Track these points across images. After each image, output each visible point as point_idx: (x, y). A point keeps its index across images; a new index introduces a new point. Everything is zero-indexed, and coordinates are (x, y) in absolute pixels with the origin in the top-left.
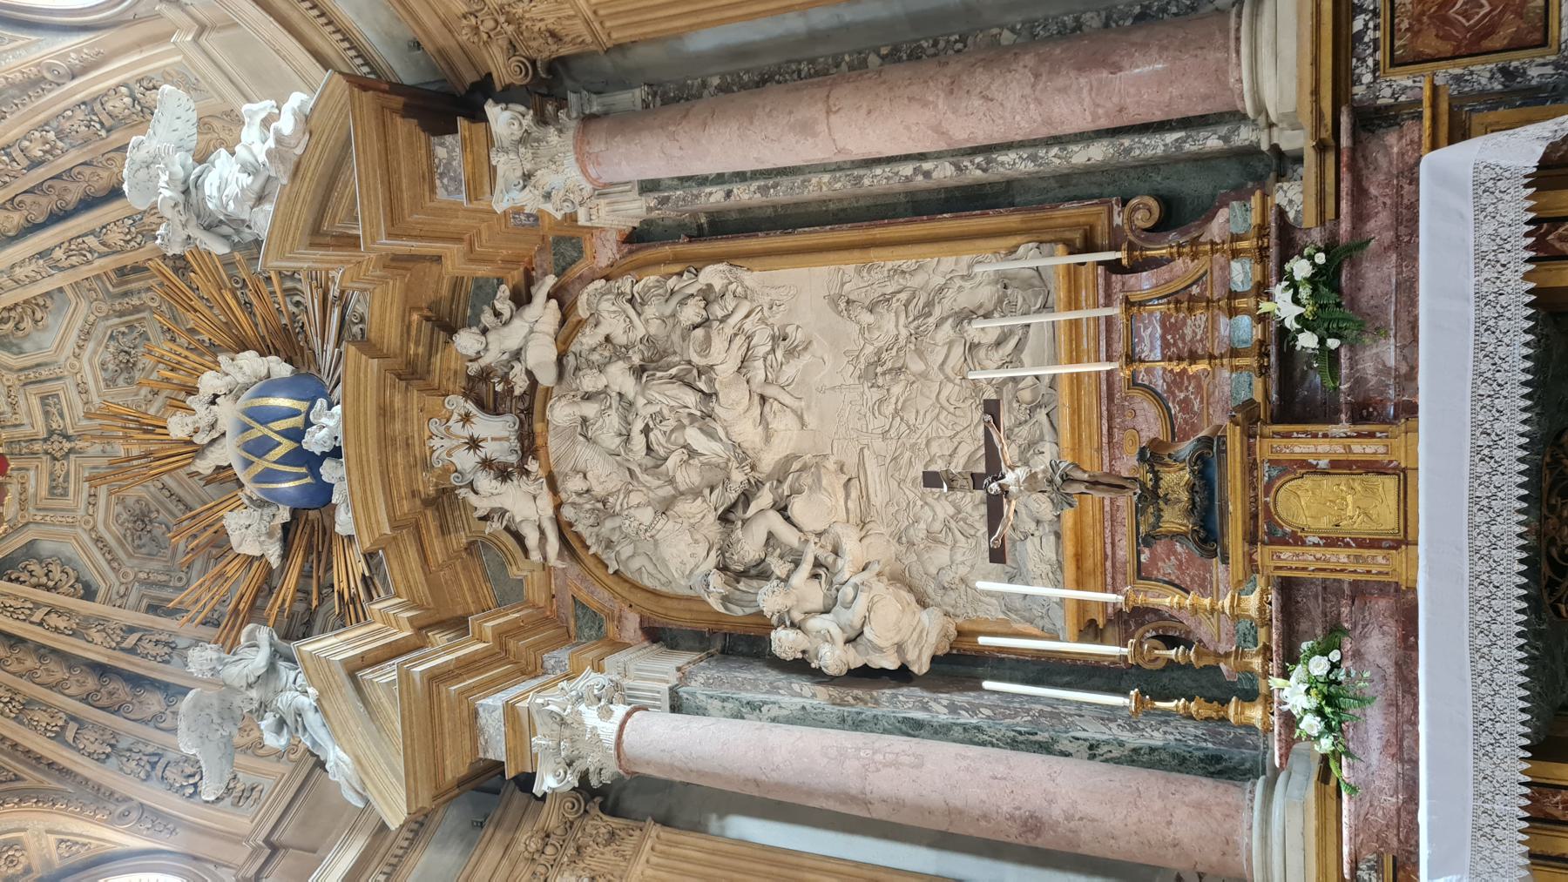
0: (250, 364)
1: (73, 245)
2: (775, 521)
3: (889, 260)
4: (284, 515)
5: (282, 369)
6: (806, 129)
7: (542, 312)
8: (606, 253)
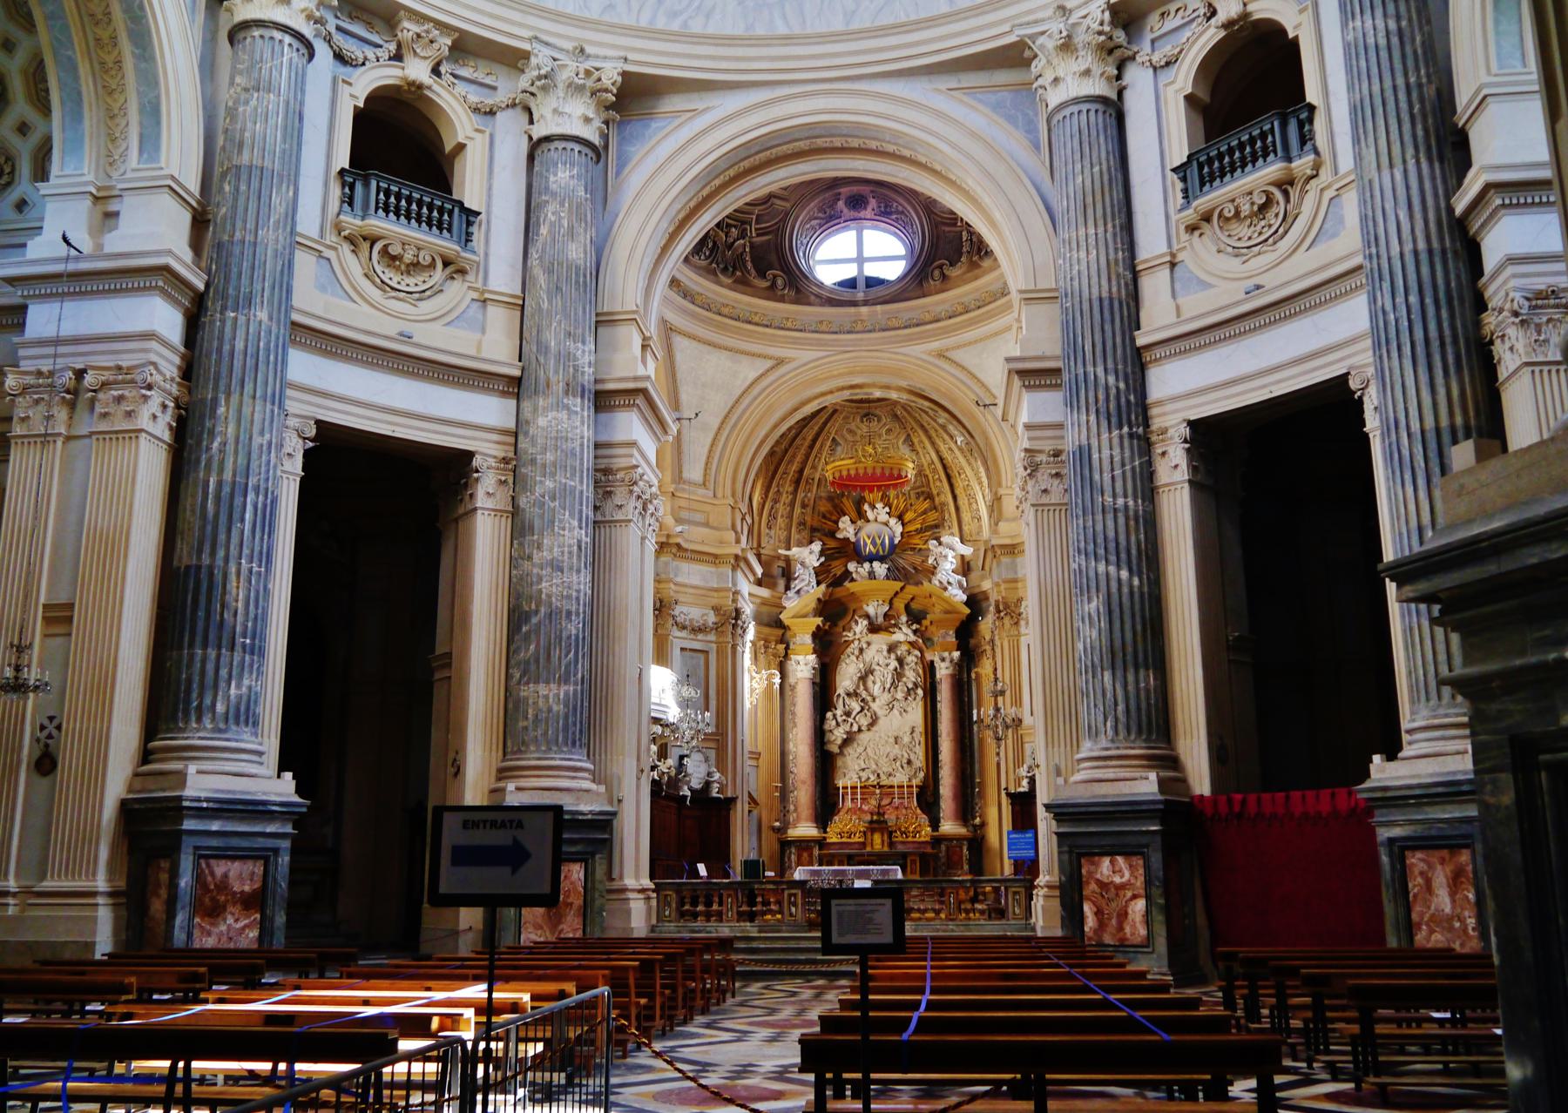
0: (899, 529)
1: (935, 471)
2: (858, 709)
3: (923, 740)
4: (853, 539)
5: (896, 541)
6: (948, 735)
7: (912, 638)
8: (928, 657)
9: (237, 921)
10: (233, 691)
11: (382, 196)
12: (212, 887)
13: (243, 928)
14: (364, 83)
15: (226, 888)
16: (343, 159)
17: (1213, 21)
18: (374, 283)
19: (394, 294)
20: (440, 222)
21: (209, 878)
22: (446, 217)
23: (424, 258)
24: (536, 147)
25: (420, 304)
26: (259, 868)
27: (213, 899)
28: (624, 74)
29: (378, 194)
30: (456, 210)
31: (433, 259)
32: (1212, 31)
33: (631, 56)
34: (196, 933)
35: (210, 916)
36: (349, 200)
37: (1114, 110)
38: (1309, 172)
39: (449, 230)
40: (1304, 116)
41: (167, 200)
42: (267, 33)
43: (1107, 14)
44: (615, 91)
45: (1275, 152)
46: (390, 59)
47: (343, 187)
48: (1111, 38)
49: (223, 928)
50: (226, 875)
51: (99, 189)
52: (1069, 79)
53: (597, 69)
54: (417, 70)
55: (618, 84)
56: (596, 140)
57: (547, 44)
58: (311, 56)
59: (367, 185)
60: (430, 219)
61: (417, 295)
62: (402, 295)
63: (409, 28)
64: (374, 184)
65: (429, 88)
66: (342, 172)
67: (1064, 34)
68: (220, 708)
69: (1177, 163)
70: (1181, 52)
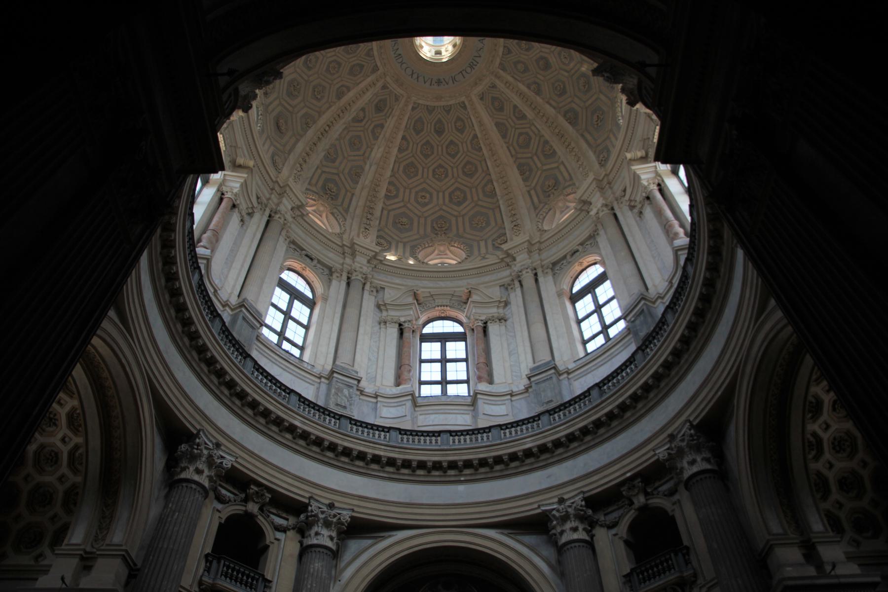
11: (225, 569)
16: (208, 550)
17: (633, 506)
20: (252, 584)
22: (255, 582)
24: (305, 551)
28: (352, 517)
29: (223, 568)
30: (261, 579)
32: (633, 511)
33: (356, 509)
36: (208, 570)
37: (590, 545)
38: (693, 579)
40: (685, 551)
41: (118, 561)
42: (189, 485)
43: (583, 503)
44: (346, 525)
45: (674, 568)
46: (241, 501)
47: (206, 563)
48: (585, 512)
51: (86, 552)
52: (568, 531)
53: (339, 514)
54: (253, 508)
55: (349, 521)
56: (334, 548)
57: (317, 501)
58: (206, 497)
59: (219, 563)
60: (247, 582)
63: (254, 488)
64: (222, 562)
65: (257, 516)
66: (207, 556)
67: (564, 510)
69: (625, 573)
70: (619, 520)
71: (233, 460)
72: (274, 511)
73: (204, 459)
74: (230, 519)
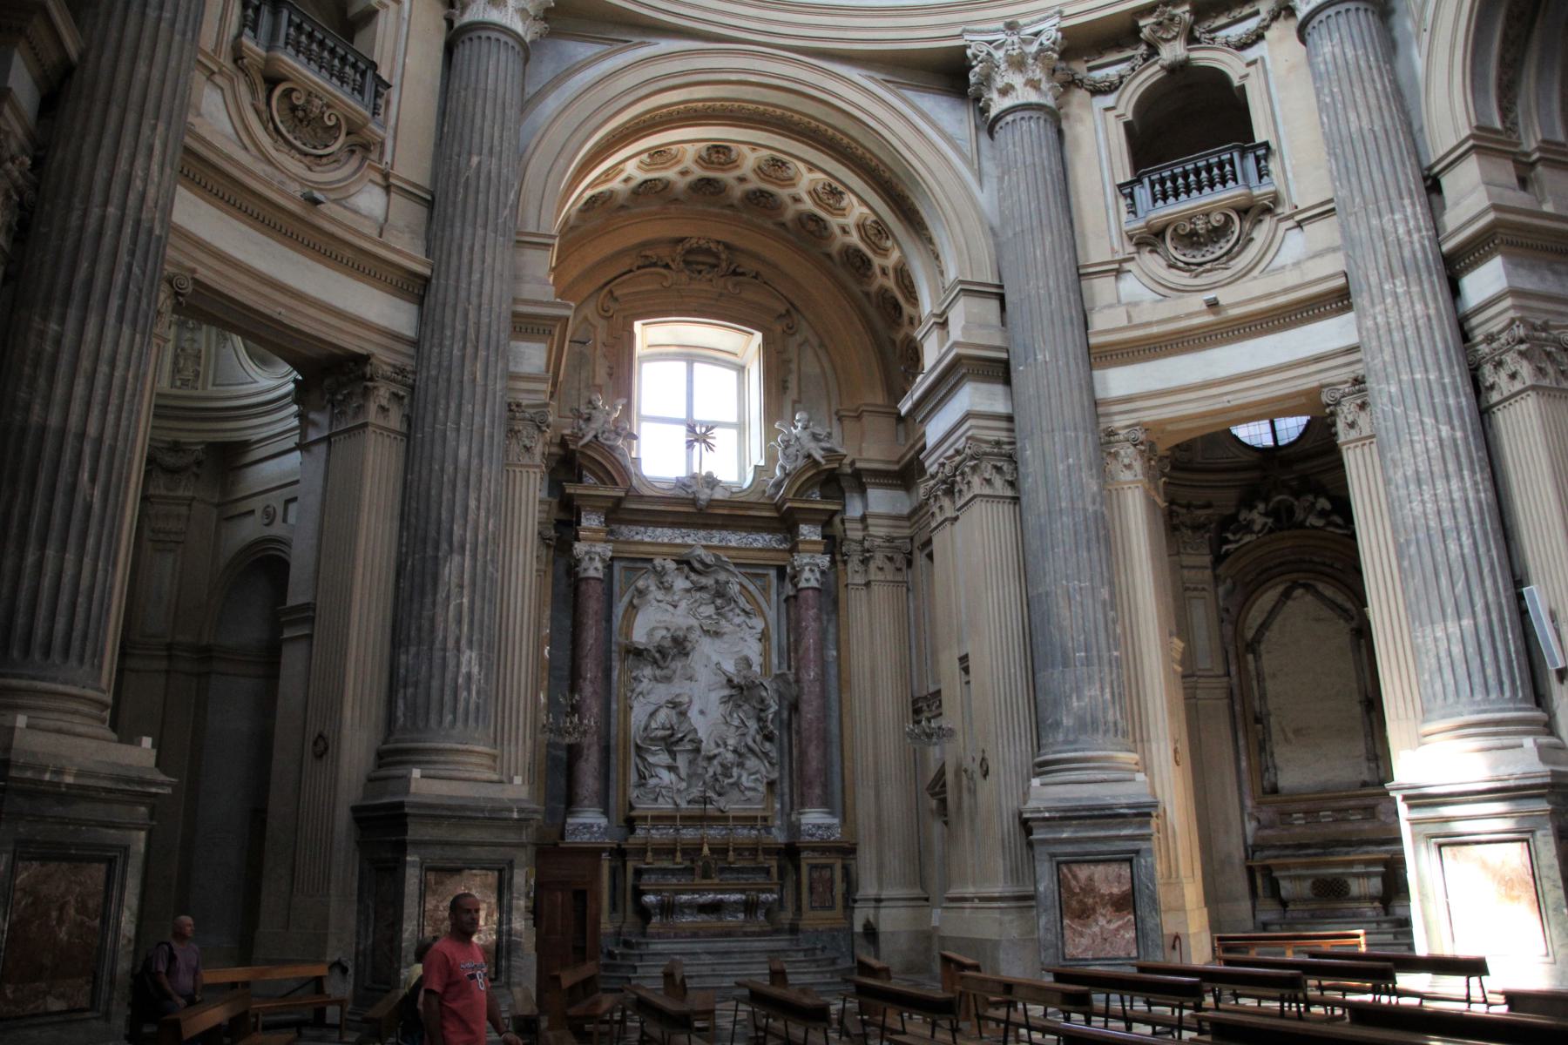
9: (1109, 922)
10: (1075, 704)
12: (1078, 890)
13: (1117, 929)
14: (1126, 102)
15: (1092, 890)
18: (1179, 269)
19: (1201, 269)
21: (1073, 883)
23: (1217, 219)
25: (1232, 263)
26: (1125, 870)
27: (1080, 902)
31: (1227, 217)
34: (1067, 933)
35: (1079, 917)
39: (1235, 179)
49: (1096, 929)
50: (1090, 879)
54: (1174, 51)
61: (1225, 258)
62: (1208, 266)
65: (1188, 60)
68: (1067, 721)
71: (1056, 20)
72: (1223, 20)
73: (1003, 67)
74: (1146, 104)
